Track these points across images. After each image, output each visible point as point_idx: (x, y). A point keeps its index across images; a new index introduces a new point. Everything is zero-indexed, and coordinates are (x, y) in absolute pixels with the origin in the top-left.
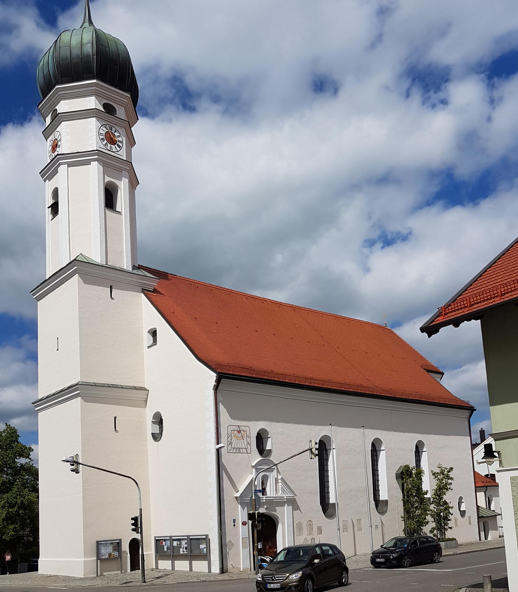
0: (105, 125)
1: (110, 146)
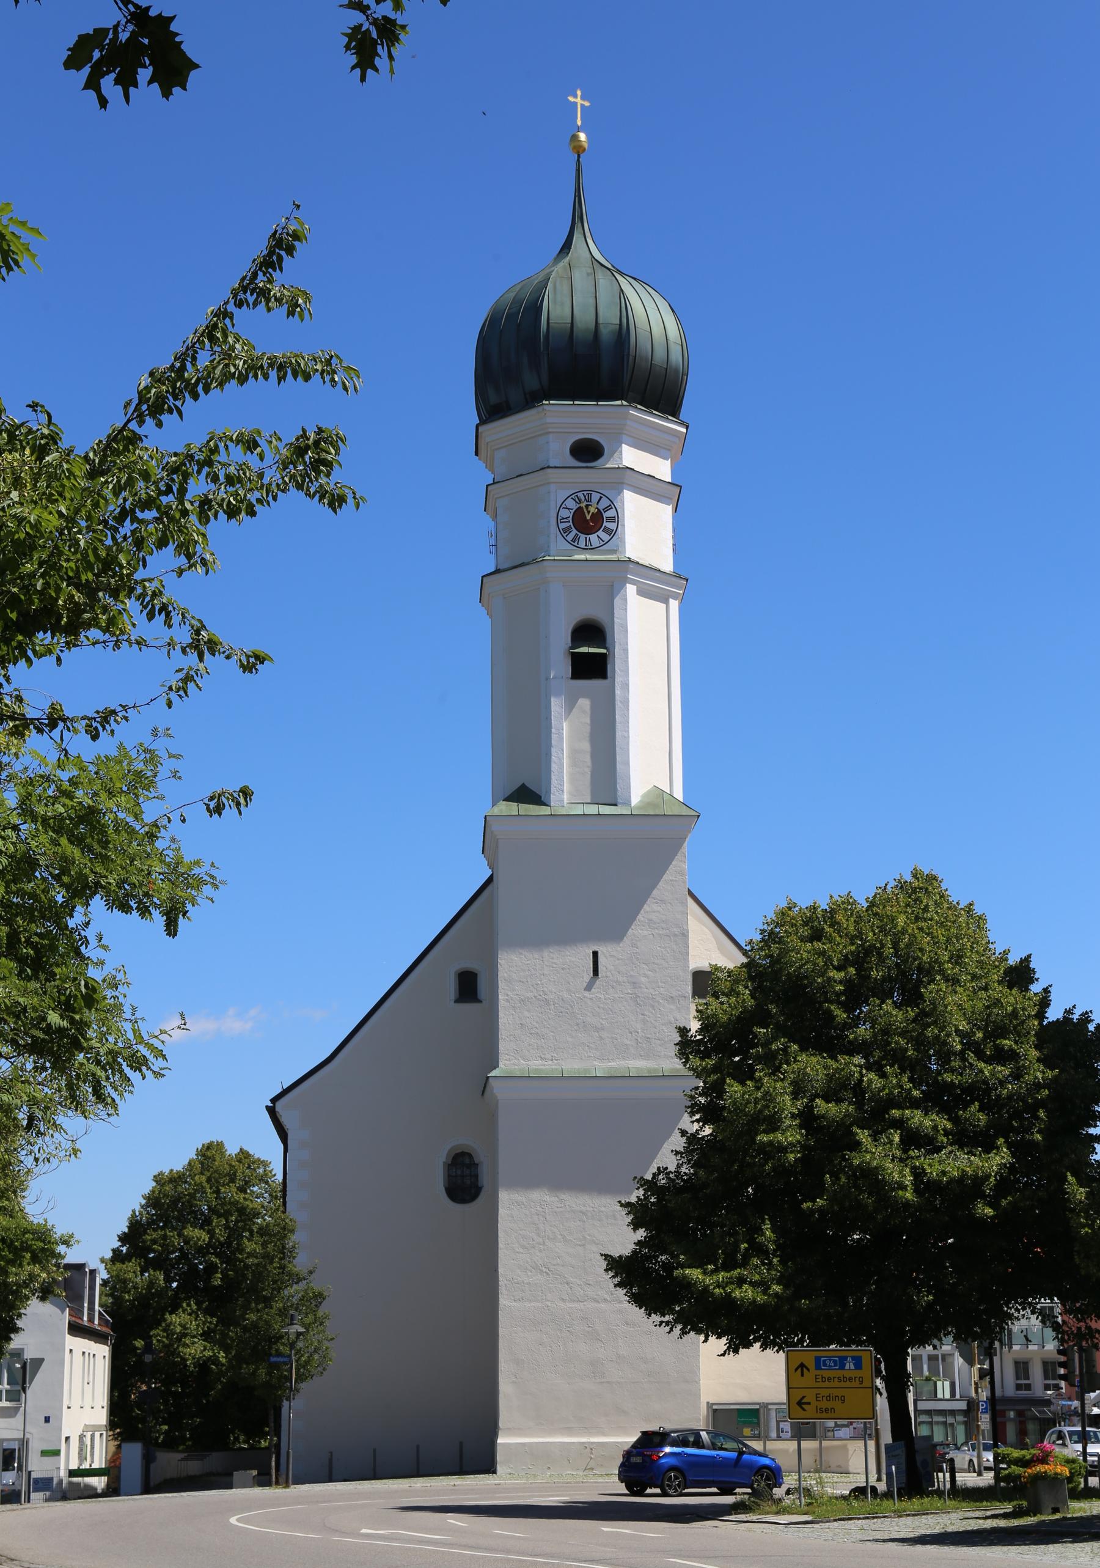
0: (573, 496)
1: (586, 538)
